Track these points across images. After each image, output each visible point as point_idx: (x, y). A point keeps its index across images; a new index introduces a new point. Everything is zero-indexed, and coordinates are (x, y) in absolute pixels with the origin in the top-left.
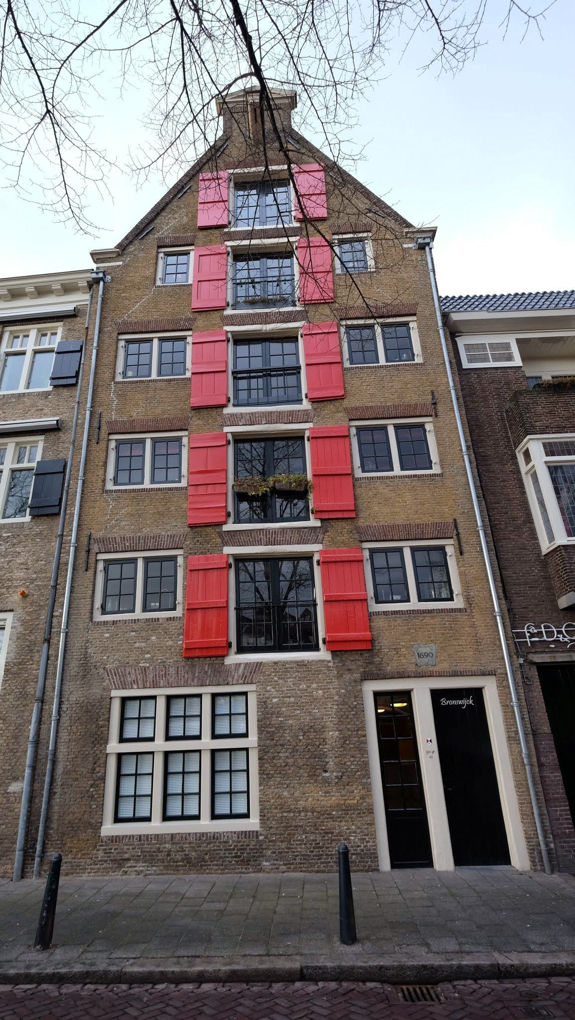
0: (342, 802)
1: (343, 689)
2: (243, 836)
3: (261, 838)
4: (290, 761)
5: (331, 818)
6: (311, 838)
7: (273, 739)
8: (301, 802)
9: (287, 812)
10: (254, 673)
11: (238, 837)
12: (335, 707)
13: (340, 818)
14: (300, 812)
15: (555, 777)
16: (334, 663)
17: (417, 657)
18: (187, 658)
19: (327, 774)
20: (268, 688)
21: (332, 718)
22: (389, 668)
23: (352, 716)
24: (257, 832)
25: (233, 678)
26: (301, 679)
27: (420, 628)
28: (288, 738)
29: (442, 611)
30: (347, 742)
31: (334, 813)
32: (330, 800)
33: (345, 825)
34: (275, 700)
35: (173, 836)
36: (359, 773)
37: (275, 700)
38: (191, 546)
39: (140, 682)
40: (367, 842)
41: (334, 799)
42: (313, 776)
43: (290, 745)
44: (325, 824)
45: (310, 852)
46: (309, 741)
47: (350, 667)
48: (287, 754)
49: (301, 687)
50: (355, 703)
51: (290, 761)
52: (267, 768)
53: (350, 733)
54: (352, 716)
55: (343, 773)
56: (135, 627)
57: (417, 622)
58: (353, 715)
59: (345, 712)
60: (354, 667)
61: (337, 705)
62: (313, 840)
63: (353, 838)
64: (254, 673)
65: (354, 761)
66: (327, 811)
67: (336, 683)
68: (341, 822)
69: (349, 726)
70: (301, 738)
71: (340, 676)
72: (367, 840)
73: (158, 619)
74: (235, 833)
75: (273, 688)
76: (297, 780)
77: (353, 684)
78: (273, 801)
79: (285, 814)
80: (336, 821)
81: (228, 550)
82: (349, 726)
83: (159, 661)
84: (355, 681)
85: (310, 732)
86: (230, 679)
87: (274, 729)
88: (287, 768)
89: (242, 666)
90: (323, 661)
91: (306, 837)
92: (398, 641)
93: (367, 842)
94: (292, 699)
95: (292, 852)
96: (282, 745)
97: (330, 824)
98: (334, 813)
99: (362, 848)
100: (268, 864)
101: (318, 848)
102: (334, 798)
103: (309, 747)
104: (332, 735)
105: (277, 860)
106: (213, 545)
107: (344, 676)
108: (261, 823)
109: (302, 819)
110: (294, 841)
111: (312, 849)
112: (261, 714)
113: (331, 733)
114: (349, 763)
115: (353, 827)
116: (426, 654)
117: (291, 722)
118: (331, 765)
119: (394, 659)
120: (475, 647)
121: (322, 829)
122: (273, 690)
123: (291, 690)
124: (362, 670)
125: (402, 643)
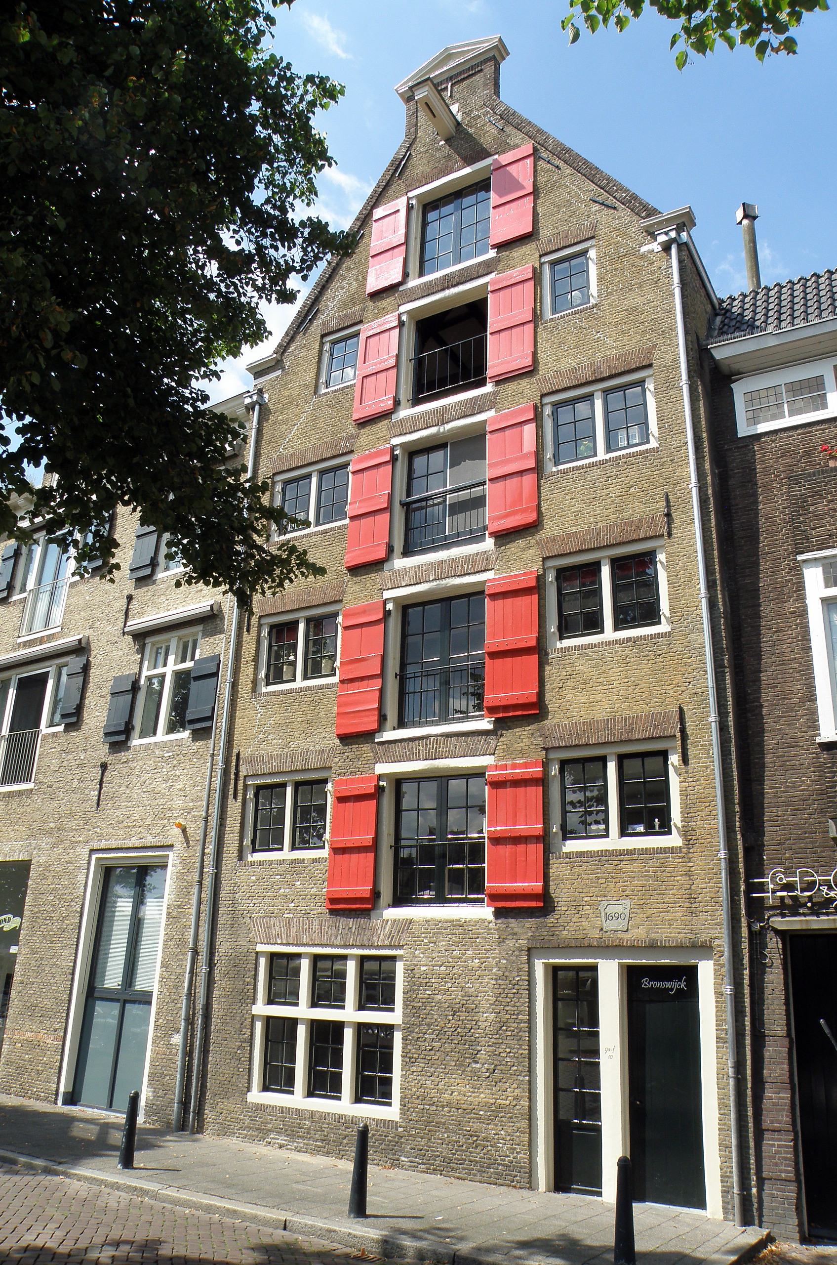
0: (492, 1101)
1: (504, 959)
2: (382, 1125)
3: (400, 1129)
4: (437, 1044)
5: (477, 1119)
6: (454, 1138)
7: (419, 1017)
8: (446, 1095)
9: (429, 1105)
10: (402, 933)
11: (377, 1126)
12: (493, 982)
13: (489, 1120)
14: (443, 1107)
15: (780, 1098)
16: (496, 924)
17: (604, 920)
18: (333, 912)
19: (478, 1066)
20: (417, 952)
21: (488, 995)
22: (565, 933)
23: (512, 996)
24: (397, 1123)
25: (379, 938)
26: (456, 944)
27: (612, 877)
28: (436, 1017)
29: (646, 851)
30: (504, 1028)
31: (481, 1113)
32: (478, 1097)
33: (493, 1129)
34: (423, 968)
35: (312, 1113)
36: (515, 1068)
37: (423, 968)
38: (340, 764)
39: (283, 937)
40: (517, 1153)
41: (483, 1096)
42: (459, 1065)
43: (437, 1026)
44: (471, 1124)
45: (452, 1154)
46: (460, 1023)
47: (516, 930)
48: (434, 1036)
49: (455, 952)
50: (517, 979)
51: (437, 1044)
52: (410, 1050)
53: (509, 1016)
54: (512, 996)
55: (496, 1065)
56: (281, 869)
57: (610, 868)
58: (514, 994)
59: (504, 989)
60: (519, 931)
61: (496, 980)
62: (456, 1142)
63: (501, 1145)
64: (402, 933)
65: (510, 1052)
66: (474, 1109)
67: (497, 951)
68: (488, 1124)
69: (507, 1008)
70: (451, 1018)
71: (502, 940)
72: (518, 1150)
73: (304, 859)
74: (374, 1120)
75: (422, 953)
76: (442, 1068)
77: (517, 953)
78: (414, 1089)
79: (428, 1107)
80: (484, 1123)
81: (382, 768)
82: (507, 1008)
83: (303, 912)
84: (520, 949)
85: (462, 1012)
86: (375, 939)
87: (420, 1004)
88: (432, 1052)
89: (390, 922)
90: (483, 921)
91: (448, 1137)
92: (581, 895)
93: (517, 1153)
94: (443, 968)
95: (432, 1151)
96: (429, 1025)
97: (477, 1125)
98: (481, 1113)
99: (511, 1158)
100: (406, 1160)
101: (461, 1151)
102: (482, 1095)
103: (459, 1030)
104: (487, 1018)
105: (416, 1157)
106: (363, 762)
107: (507, 942)
108: (401, 1113)
109: (445, 1115)
110: (435, 1139)
111: (454, 1151)
112: (407, 984)
113: (485, 1015)
114: (505, 1055)
115: (502, 1133)
116: (617, 915)
117: (440, 997)
118: (483, 1055)
119: (574, 920)
120: (687, 905)
121: (466, 1130)
122: (421, 955)
123: (443, 957)
124: (530, 934)
125: (586, 899)
